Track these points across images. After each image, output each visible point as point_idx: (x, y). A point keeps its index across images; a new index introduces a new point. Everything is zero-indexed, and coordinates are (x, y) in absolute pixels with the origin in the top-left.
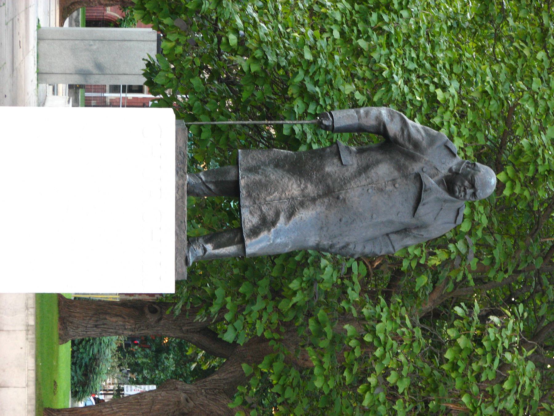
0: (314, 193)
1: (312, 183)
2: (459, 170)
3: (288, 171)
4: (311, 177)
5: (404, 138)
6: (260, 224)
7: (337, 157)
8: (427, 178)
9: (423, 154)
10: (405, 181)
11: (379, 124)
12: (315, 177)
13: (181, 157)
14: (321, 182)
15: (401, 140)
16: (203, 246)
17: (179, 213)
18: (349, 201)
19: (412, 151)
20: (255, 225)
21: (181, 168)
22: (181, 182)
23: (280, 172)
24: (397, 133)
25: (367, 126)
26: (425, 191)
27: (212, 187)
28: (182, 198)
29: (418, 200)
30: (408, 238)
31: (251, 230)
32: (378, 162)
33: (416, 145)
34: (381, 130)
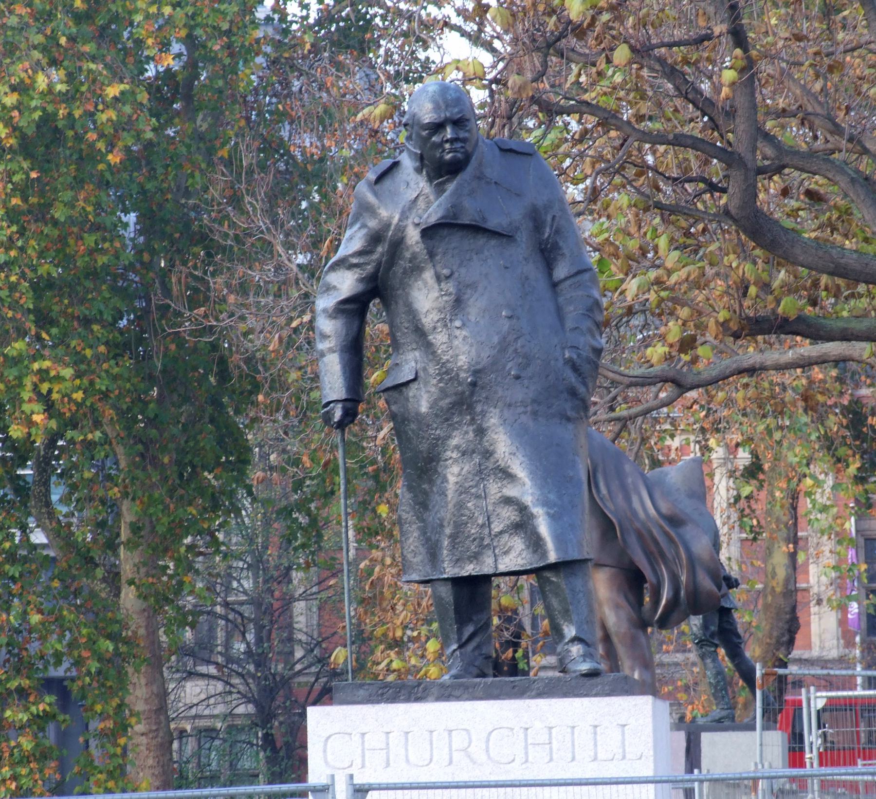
0: (467, 433)
1: (449, 437)
2: (416, 154)
3: (431, 482)
4: (438, 439)
5: (368, 264)
6: (526, 533)
12: (438, 432)
14: (447, 420)
15: (370, 268)
16: (567, 643)
17: (496, 692)
18: (478, 363)
19: (386, 246)
21: (410, 693)
24: (356, 276)
25: (347, 335)
27: (469, 629)
28: (466, 688)
29: (476, 229)
30: (561, 244)
32: (412, 313)
33: (375, 238)
34: (354, 309)
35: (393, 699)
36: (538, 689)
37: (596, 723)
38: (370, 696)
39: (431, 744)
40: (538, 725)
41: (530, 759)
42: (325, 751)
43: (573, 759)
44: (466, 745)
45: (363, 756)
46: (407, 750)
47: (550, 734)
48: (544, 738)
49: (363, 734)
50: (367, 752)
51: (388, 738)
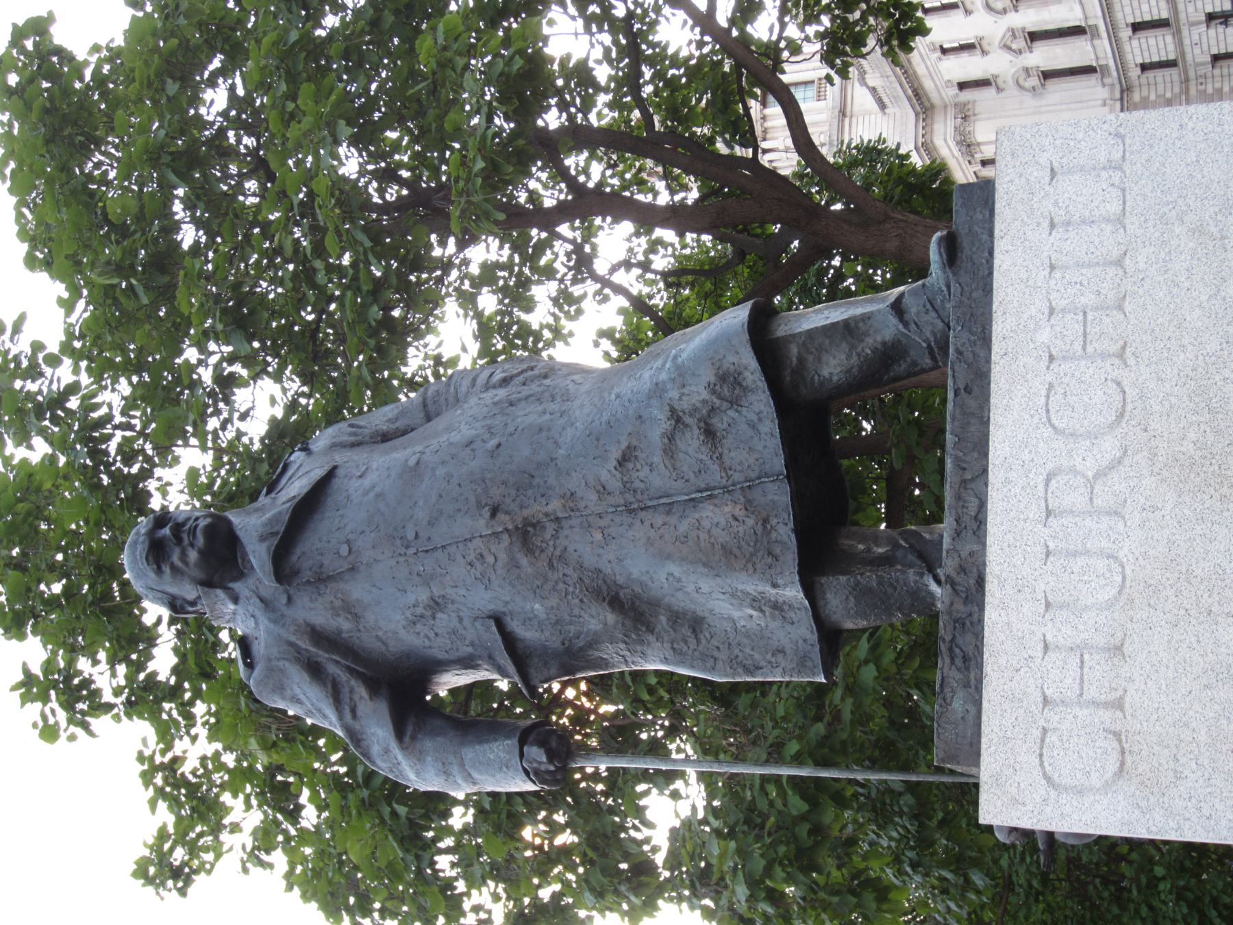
3: (655, 604)
5: (352, 691)
7: (520, 645)
8: (261, 567)
9: (291, 644)
10: (326, 562)
11: (413, 738)
13: (966, 641)
15: (362, 691)
16: (906, 325)
22: (967, 547)
23: (680, 601)
26: (273, 534)
33: (315, 671)
37: (1046, 224)
38: (967, 685)
39: (1075, 554)
42: (1080, 791)
45: (1095, 703)
47: (1063, 310)
49: (1046, 701)
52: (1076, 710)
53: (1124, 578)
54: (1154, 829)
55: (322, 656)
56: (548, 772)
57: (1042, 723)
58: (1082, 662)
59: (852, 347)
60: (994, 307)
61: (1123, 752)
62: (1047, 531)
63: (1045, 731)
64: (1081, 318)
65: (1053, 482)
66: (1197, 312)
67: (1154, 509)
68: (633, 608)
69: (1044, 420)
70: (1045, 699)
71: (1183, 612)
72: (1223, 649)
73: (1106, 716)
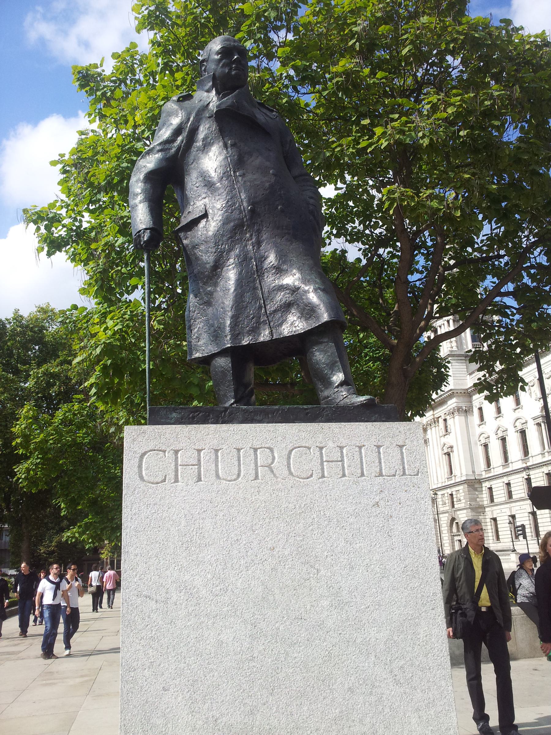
3: (216, 284)
12: (224, 246)
16: (337, 387)
20: (298, 315)
31: (307, 319)
35: (204, 421)
36: (327, 415)
40: (331, 444)
41: (326, 474)
42: (140, 467)
43: (362, 475)
44: (270, 461)
45: (176, 471)
46: (217, 466)
48: (336, 455)
49: (176, 452)
50: (180, 468)
51: (199, 455)
52: (173, 464)
53: (230, 481)
54: (126, 496)
55: (185, 134)
56: (140, 241)
57: (168, 450)
58: (194, 465)
59: (327, 365)
60: (342, 423)
61: (157, 483)
62: (248, 449)
63: (164, 451)
64: (339, 459)
65: (268, 450)
66: (342, 507)
67: (259, 492)
68: (214, 276)
69: (295, 446)
70: (179, 451)
71: (217, 504)
72: (201, 521)
73: (172, 476)
